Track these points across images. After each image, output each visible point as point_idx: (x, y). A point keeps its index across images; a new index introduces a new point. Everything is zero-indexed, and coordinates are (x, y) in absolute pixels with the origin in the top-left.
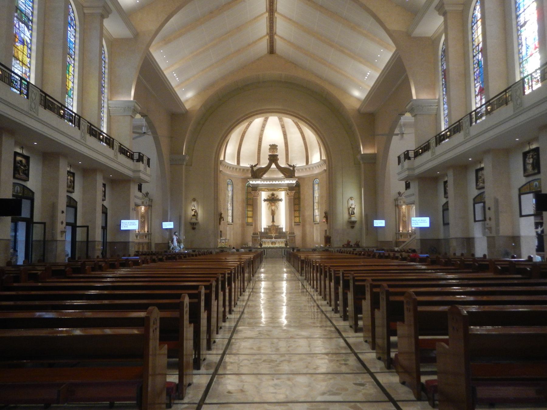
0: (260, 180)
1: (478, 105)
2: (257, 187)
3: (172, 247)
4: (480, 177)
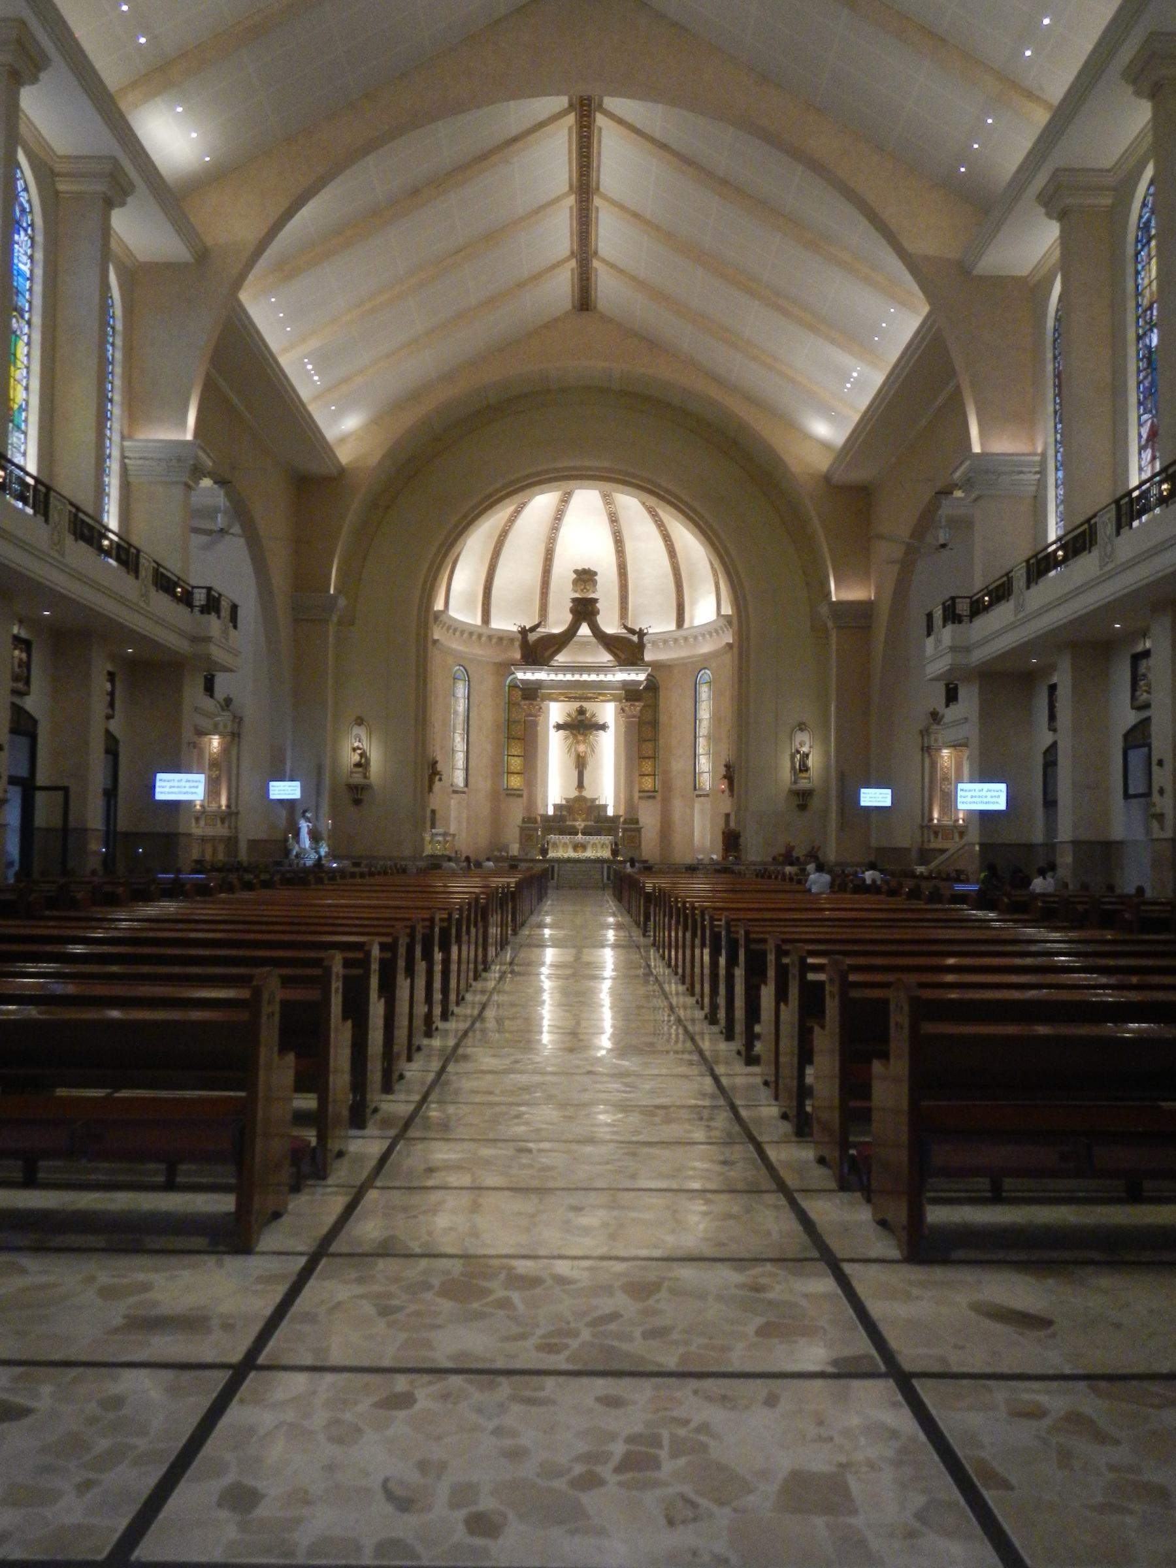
1: (1145, 476)
2: (536, 690)
3: (294, 853)
4: (1144, 675)
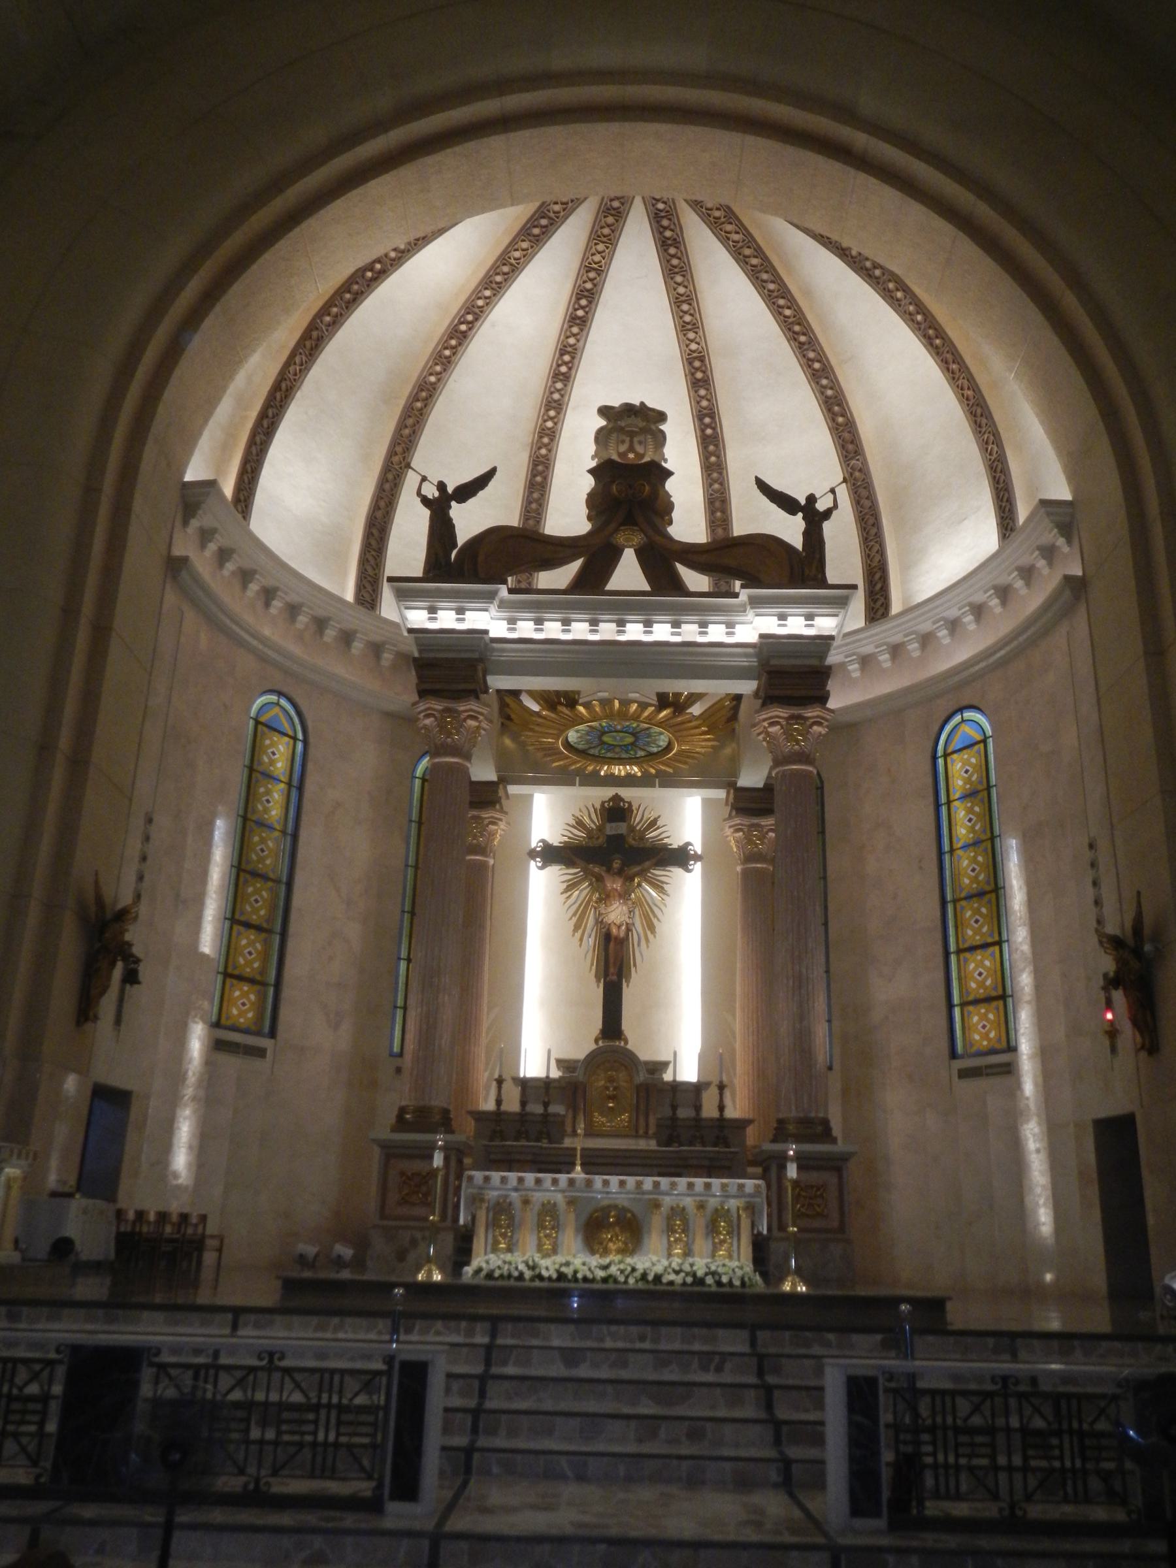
0: (503, 605)
